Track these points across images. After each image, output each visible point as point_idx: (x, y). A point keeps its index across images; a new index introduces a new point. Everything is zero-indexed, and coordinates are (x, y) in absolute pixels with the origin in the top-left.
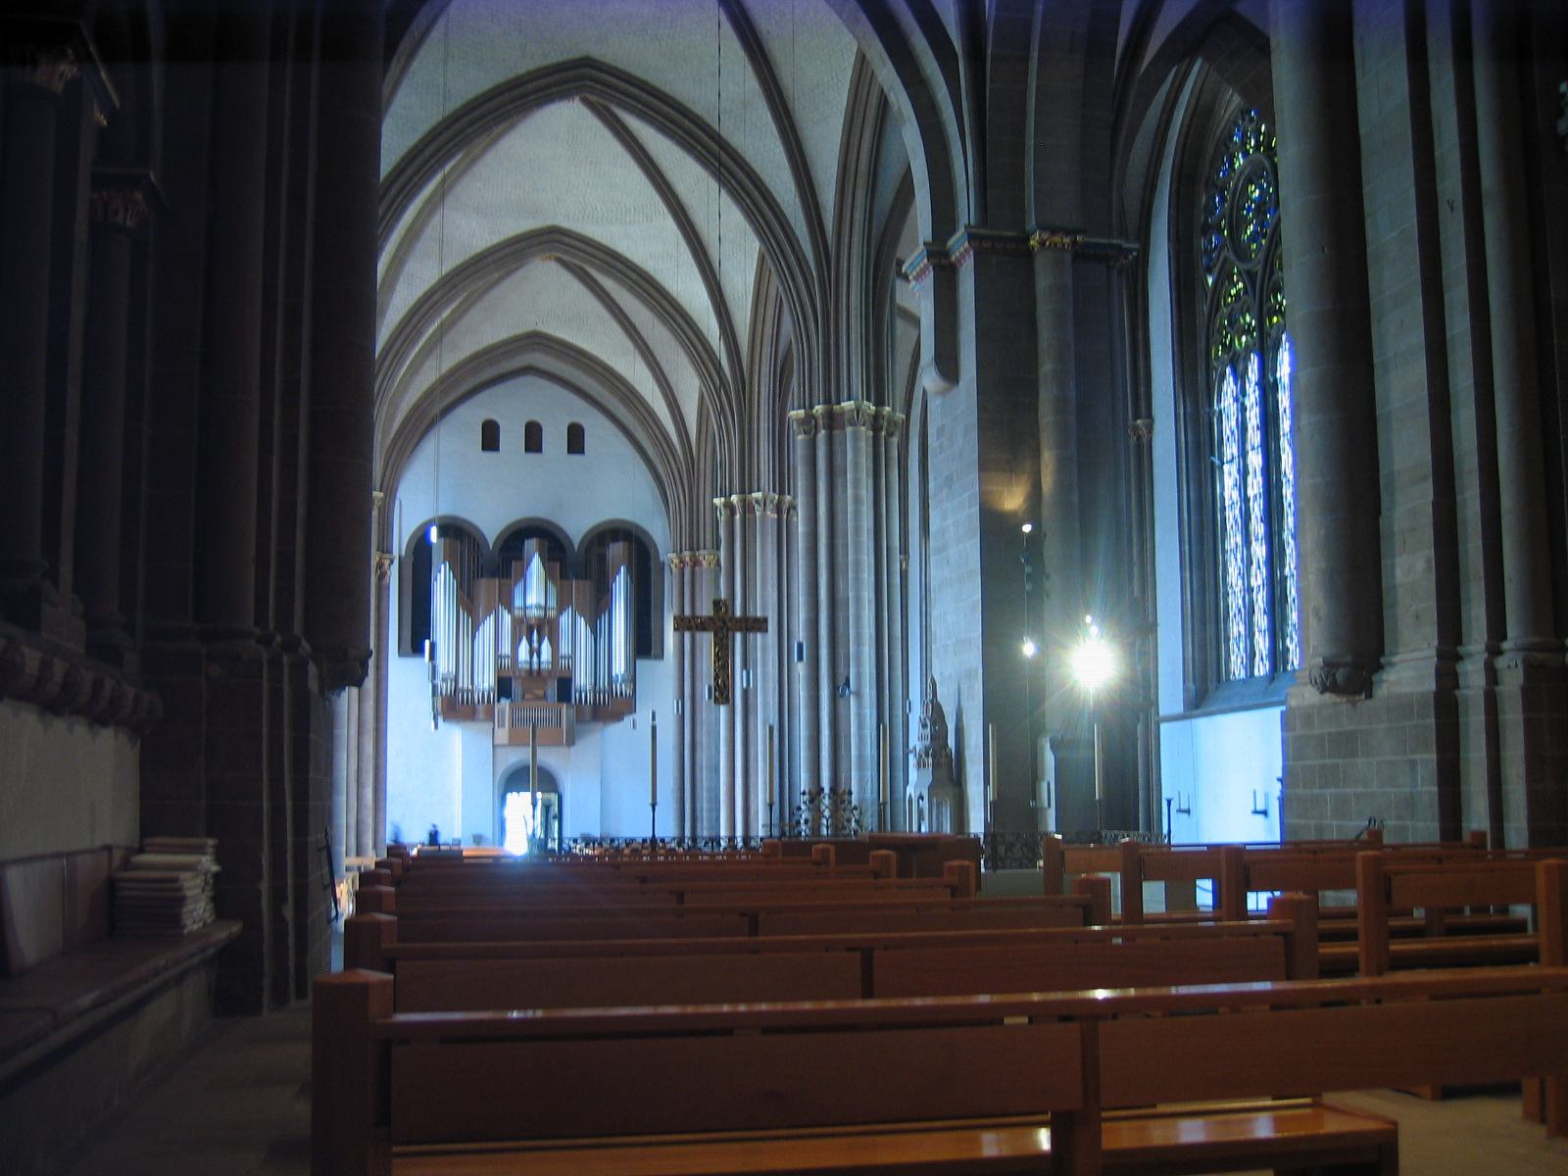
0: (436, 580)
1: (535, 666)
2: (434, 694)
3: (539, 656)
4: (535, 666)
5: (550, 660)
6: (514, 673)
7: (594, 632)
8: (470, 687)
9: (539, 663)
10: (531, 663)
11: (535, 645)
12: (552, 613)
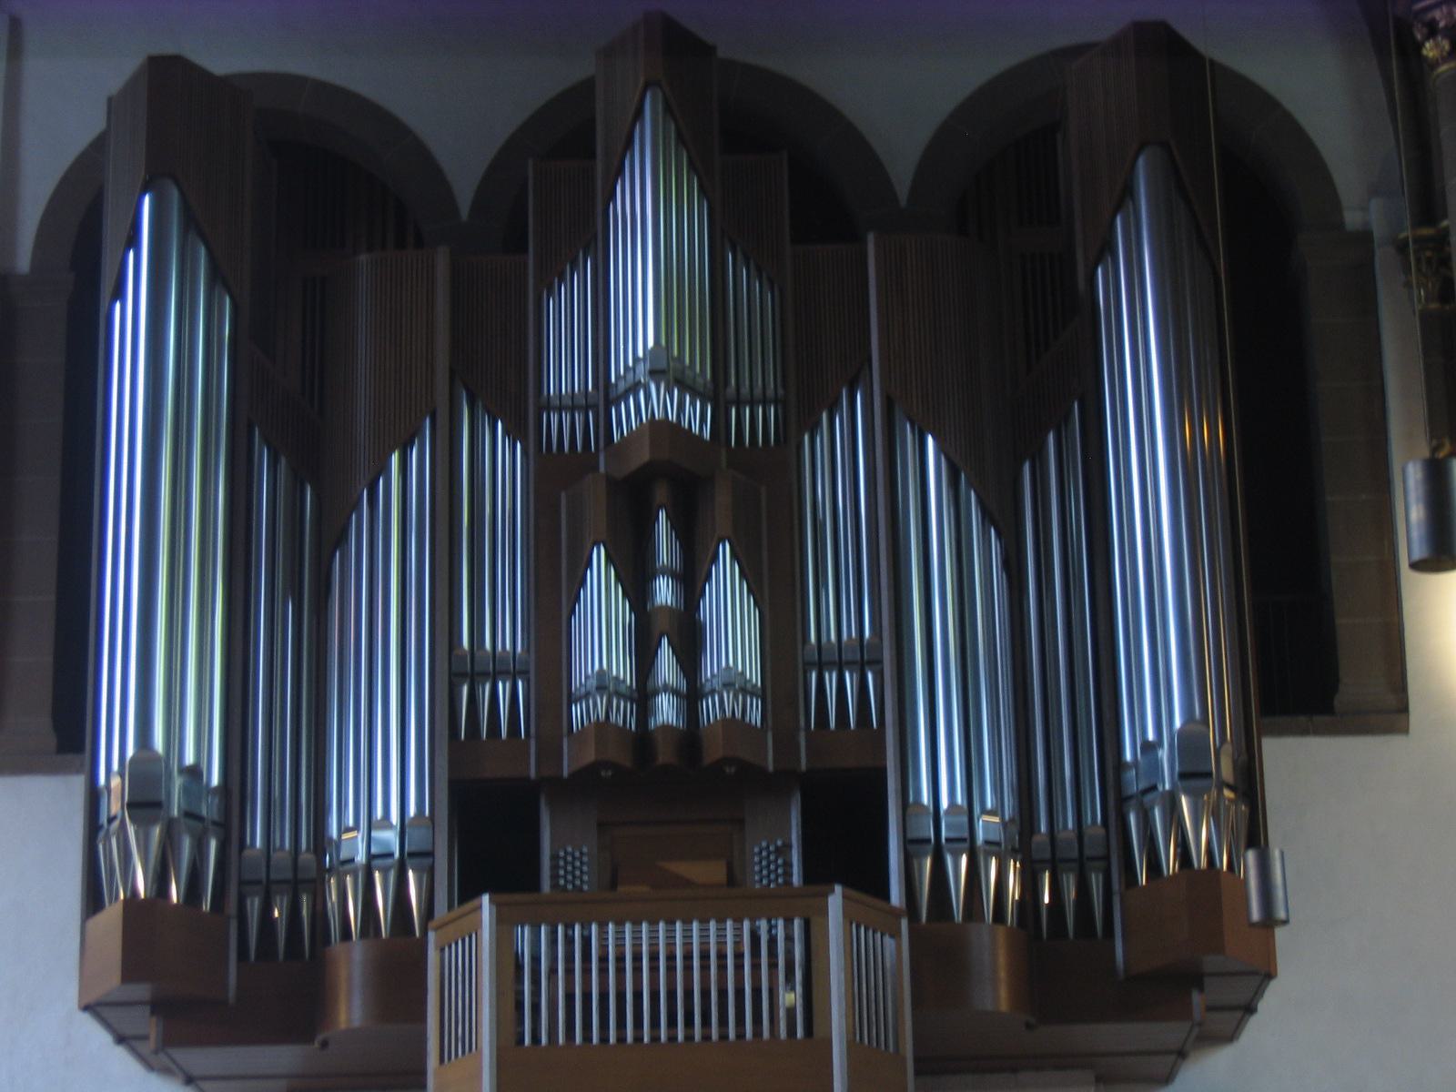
0: (119, 293)
1: (666, 710)
2: (93, 900)
3: (690, 655)
4: (666, 710)
5: (754, 675)
6: (550, 751)
7: (1004, 518)
8: (306, 857)
9: (692, 696)
10: (643, 696)
11: (664, 592)
12: (758, 422)
